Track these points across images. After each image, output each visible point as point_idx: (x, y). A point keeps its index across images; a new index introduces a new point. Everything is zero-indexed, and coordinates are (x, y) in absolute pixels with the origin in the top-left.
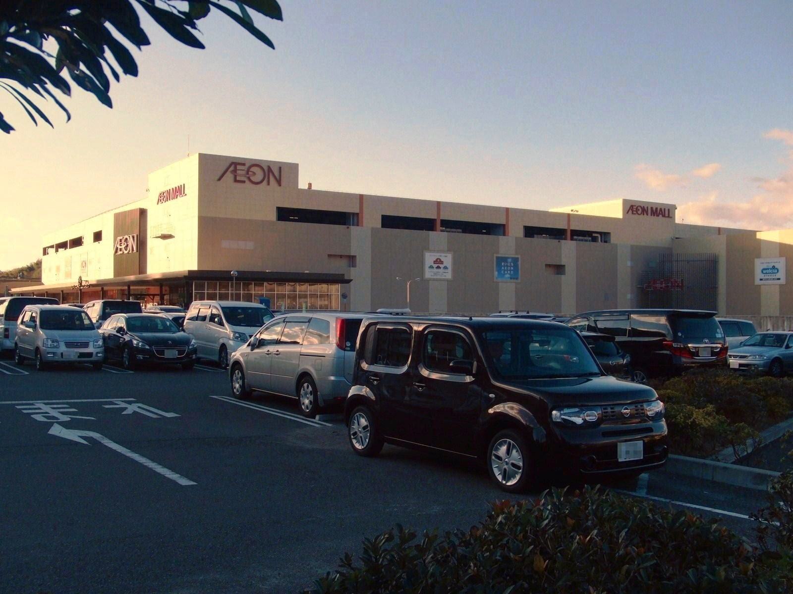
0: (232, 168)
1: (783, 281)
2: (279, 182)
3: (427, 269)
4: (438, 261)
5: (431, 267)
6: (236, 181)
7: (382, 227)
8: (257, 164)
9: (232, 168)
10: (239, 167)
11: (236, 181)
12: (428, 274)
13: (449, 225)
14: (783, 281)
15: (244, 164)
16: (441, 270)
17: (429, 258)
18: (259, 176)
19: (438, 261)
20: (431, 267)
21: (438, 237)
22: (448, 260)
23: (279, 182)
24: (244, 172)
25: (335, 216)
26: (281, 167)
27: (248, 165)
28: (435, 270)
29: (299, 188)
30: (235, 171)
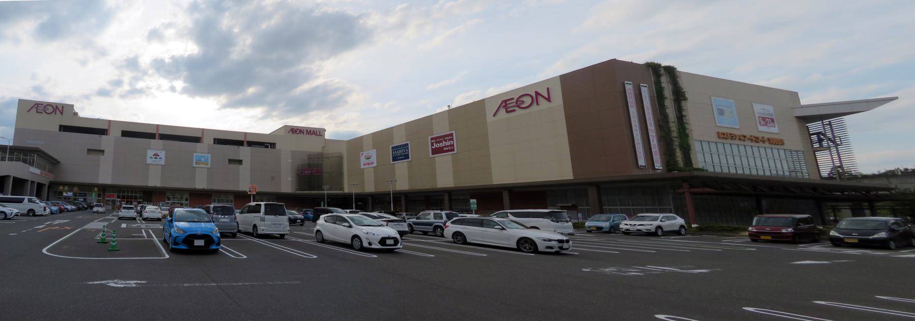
1: (375, 165)
25: (97, 130)
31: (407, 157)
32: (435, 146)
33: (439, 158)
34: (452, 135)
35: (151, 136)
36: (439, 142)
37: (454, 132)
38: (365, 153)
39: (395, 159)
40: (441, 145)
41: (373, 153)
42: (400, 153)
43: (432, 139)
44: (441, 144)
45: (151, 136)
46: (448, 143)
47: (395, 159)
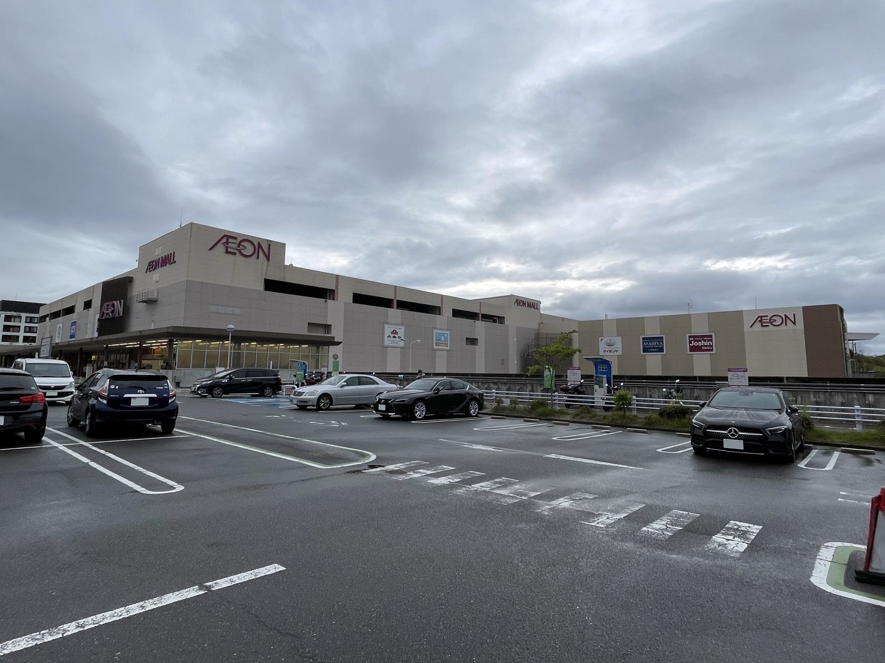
0: (224, 240)
1: (620, 353)
2: (268, 258)
3: (386, 338)
4: (394, 332)
5: (389, 336)
6: (227, 252)
7: (354, 302)
8: (248, 240)
9: (224, 240)
10: (230, 240)
11: (227, 252)
12: (387, 342)
13: (402, 305)
14: (620, 353)
15: (236, 238)
16: (397, 339)
17: (388, 329)
18: (249, 250)
19: (394, 332)
20: (389, 336)
21: (394, 313)
22: (401, 332)
23: (268, 258)
24: (235, 246)
26: (270, 243)
27: (239, 240)
28: (392, 339)
29: (287, 263)
30: (227, 242)
31: (661, 350)
32: (693, 344)
33: (697, 355)
34: (711, 336)
35: (385, 303)
36: (698, 341)
37: (713, 334)
38: (606, 339)
39: (646, 350)
40: (700, 344)
41: (618, 342)
42: (653, 345)
43: (690, 337)
44: (699, 344)
45: (385, 303)
46: (707, 343)
47: (646, 350)
